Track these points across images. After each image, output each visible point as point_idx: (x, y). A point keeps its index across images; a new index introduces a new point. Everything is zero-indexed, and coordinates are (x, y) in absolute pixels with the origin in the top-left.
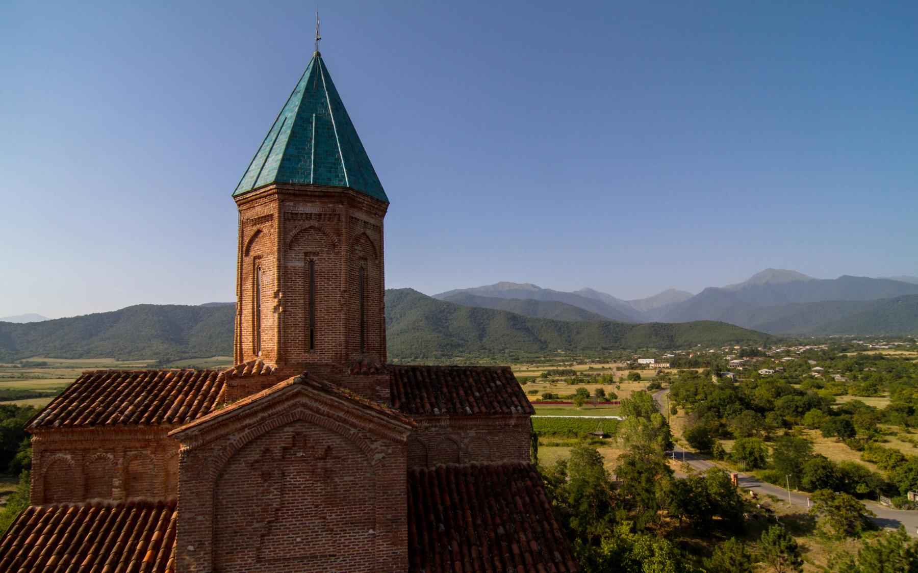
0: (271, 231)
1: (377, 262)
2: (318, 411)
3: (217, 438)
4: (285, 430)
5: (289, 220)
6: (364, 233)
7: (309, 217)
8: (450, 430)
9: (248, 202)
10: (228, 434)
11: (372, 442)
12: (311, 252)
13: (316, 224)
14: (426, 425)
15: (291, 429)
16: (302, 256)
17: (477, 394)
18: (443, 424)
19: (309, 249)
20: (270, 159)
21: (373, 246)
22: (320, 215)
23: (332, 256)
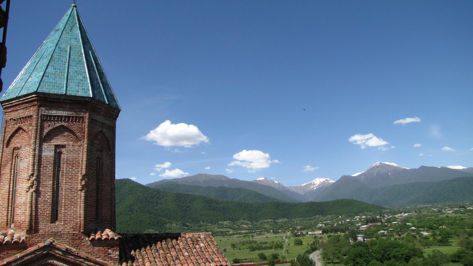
0: (31, 128)
5: (45, 120)
7: (60, 118)
9: (13, 106)
12: (59, 145)
13: (66, 124)
17: (186, 254)
19: (59, 143)
21: (108, 141)
23: (76, 148)
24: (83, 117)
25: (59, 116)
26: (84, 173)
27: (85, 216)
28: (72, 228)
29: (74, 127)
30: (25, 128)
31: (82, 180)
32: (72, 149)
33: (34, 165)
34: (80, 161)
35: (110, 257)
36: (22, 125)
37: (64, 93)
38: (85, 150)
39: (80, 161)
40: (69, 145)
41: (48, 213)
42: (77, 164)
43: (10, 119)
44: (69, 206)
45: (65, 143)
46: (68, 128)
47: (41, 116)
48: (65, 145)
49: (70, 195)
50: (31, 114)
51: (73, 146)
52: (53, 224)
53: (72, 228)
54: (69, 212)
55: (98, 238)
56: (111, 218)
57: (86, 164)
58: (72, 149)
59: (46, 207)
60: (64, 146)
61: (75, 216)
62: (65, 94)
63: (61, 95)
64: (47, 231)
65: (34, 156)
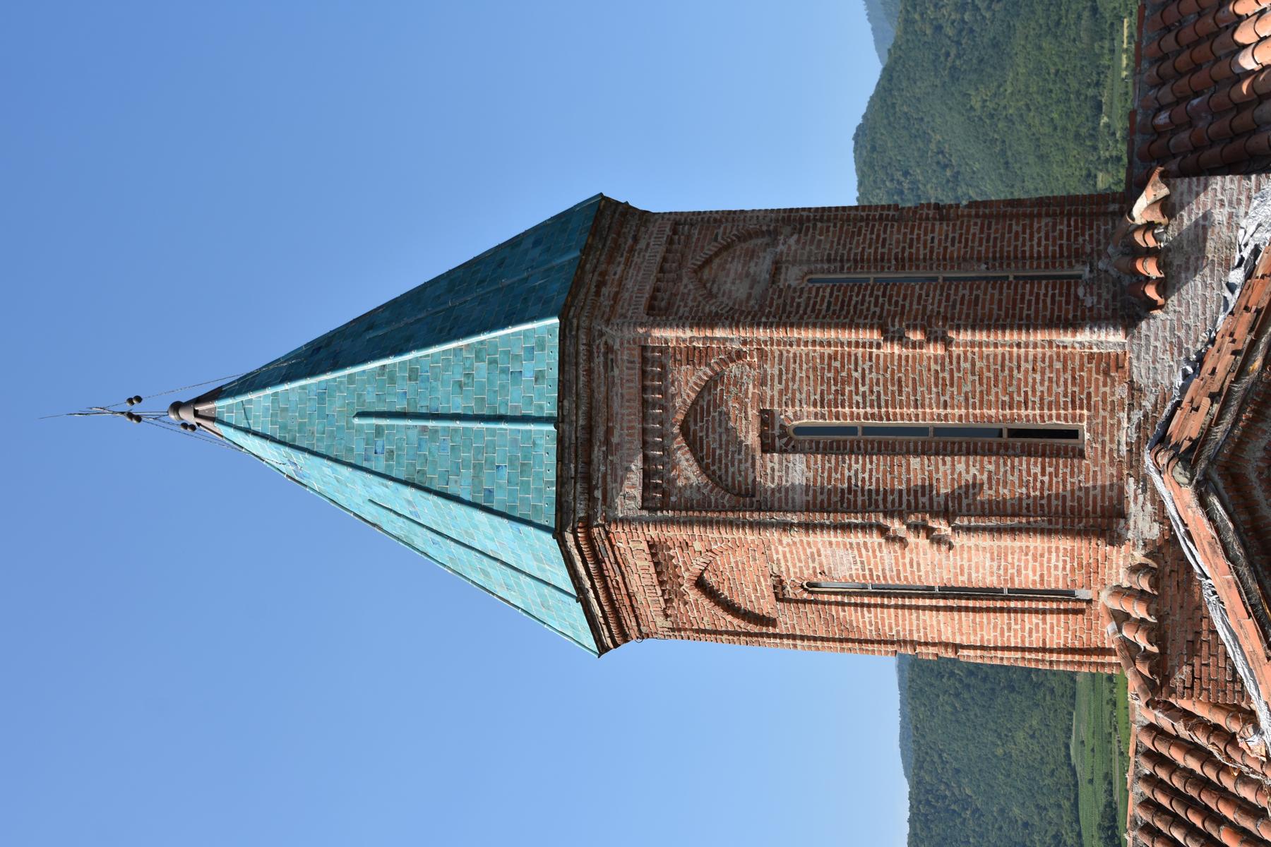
9: (616, 611)
12: (762, 435)
20: (490, 547)
26: (876, 336)
27: (1066, 328)
28: (1106, 373)
29: (686, 384)
30: (696, 567)
31: (901, 339)
32: (777, 387)
33: (846, 528)
34: (828, 351)
36: (686, 575)
37: (551, 428)
38: (779, 334)
39: (828, 351)
40: (762, 399)
41: (1038, 470)
42: (838, 364)
43: (667, 616)
44: (1013, 389)
45: (753, 413)
47: (652, 510)
48: (762, 412)
49: (967, 388)
50: (644, 546)
51: (763, 383)
52: (1088, 451)
53: (1106, 373)
55: (1159, 268)
57: (837, 326)
58: (777, 387)
60: (766, 418)
61: (1058, 365)
62: (557, 421)
63: (560, 440)
65: (808, 527)
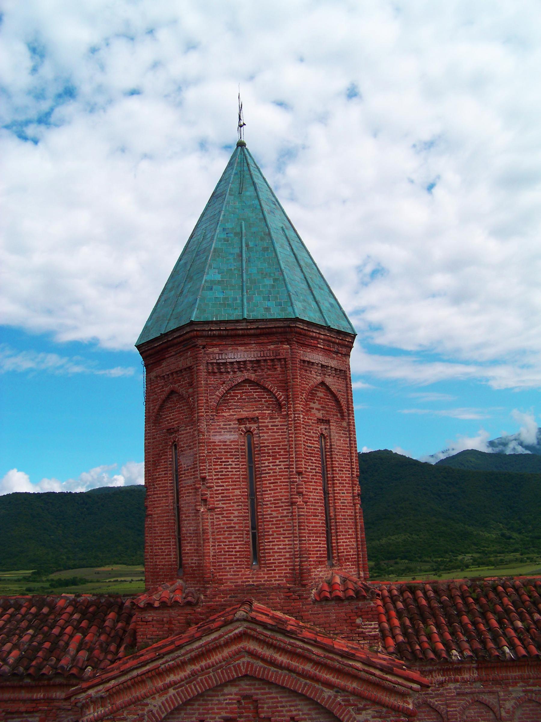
1: (344, 424)
2: (272, 663)
3: (130, 703)
4: (226, 691)
6: (323, 383)
7: (242, 365)
8: (479, 686)
10: (146, 696)
11: (359, 711)
12: (247, 418)
13: (253, 377)
14: (441, 678)
15: (234, 690)
16: (234, 424)
17: (519, 624)
18: (466, 676)
19: (244, 414)
21: (337, 401)
22: (258, 361)
23: (278, 421)
24: (285, 359)
25: (238, 362)
30: (182, 391)
35: (362, 632)
36: (176, 386)
41: (237, 549)
43: (156, 377)
44: (275, 536)
46: (258, 385)
49: (274, 514)
50: (189, 364)
54: (276, 547)
56: (358, 555)
58: (270, 424)
59: (233, 539)
64: (239, 582)
